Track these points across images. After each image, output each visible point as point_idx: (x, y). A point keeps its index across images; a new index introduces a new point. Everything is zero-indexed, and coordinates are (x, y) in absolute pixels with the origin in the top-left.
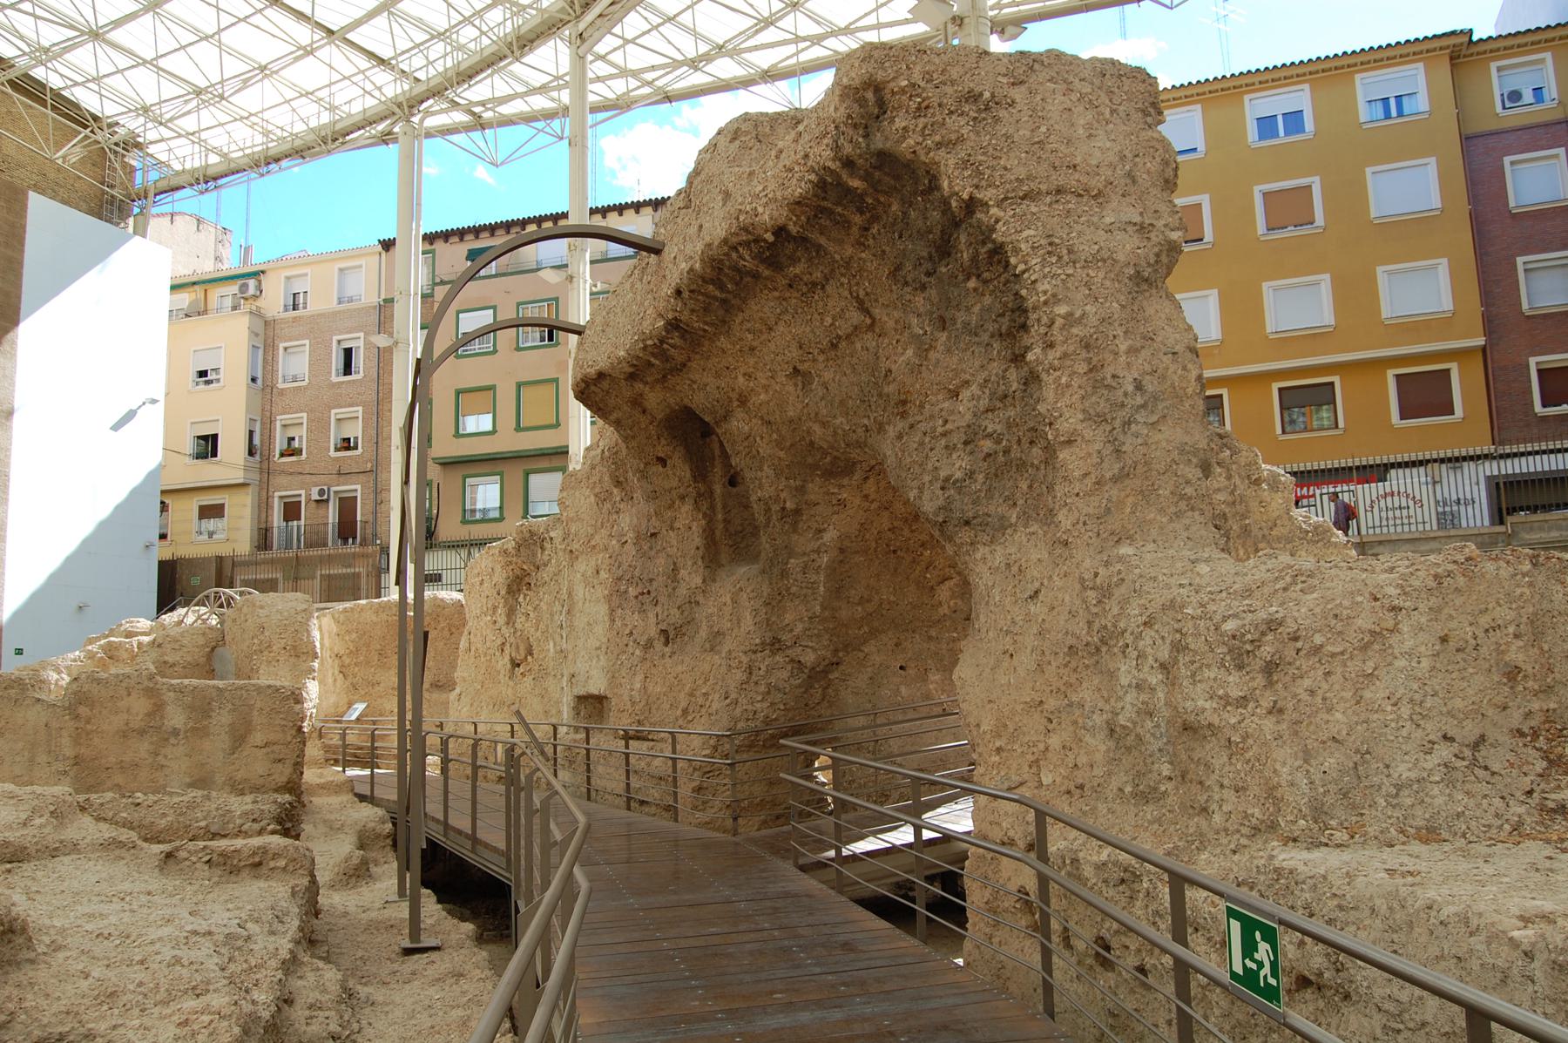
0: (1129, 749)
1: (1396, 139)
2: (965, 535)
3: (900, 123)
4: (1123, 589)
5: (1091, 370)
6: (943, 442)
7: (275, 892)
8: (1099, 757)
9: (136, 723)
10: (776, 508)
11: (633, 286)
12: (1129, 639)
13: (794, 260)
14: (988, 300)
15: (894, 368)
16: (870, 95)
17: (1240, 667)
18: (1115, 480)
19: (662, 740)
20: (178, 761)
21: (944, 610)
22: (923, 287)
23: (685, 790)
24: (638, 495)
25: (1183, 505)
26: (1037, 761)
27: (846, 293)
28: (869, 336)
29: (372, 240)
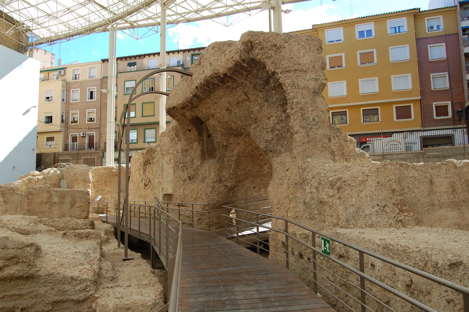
0: (308, 207)
1: (398, 39)
2: (271, 154)
3: (256, 52)
4: (308, 169)
6: (266, 130)
7: (92, 243)
8: (301, 209)
9: (44, 200)
10: (221, 144)
11: (183, 84)
13: (228, 82)
14: (277, 96)
15: (254, 111)
16: (249, 44)
17: (332, 188)
18: (307, 142)
20: (56, 210)
21: (265, 172)
22: (262, 91)
23: (195, 219)
24: (182, 139)
25: (324, 149)
28: (247, 102)
29: (99, 59)
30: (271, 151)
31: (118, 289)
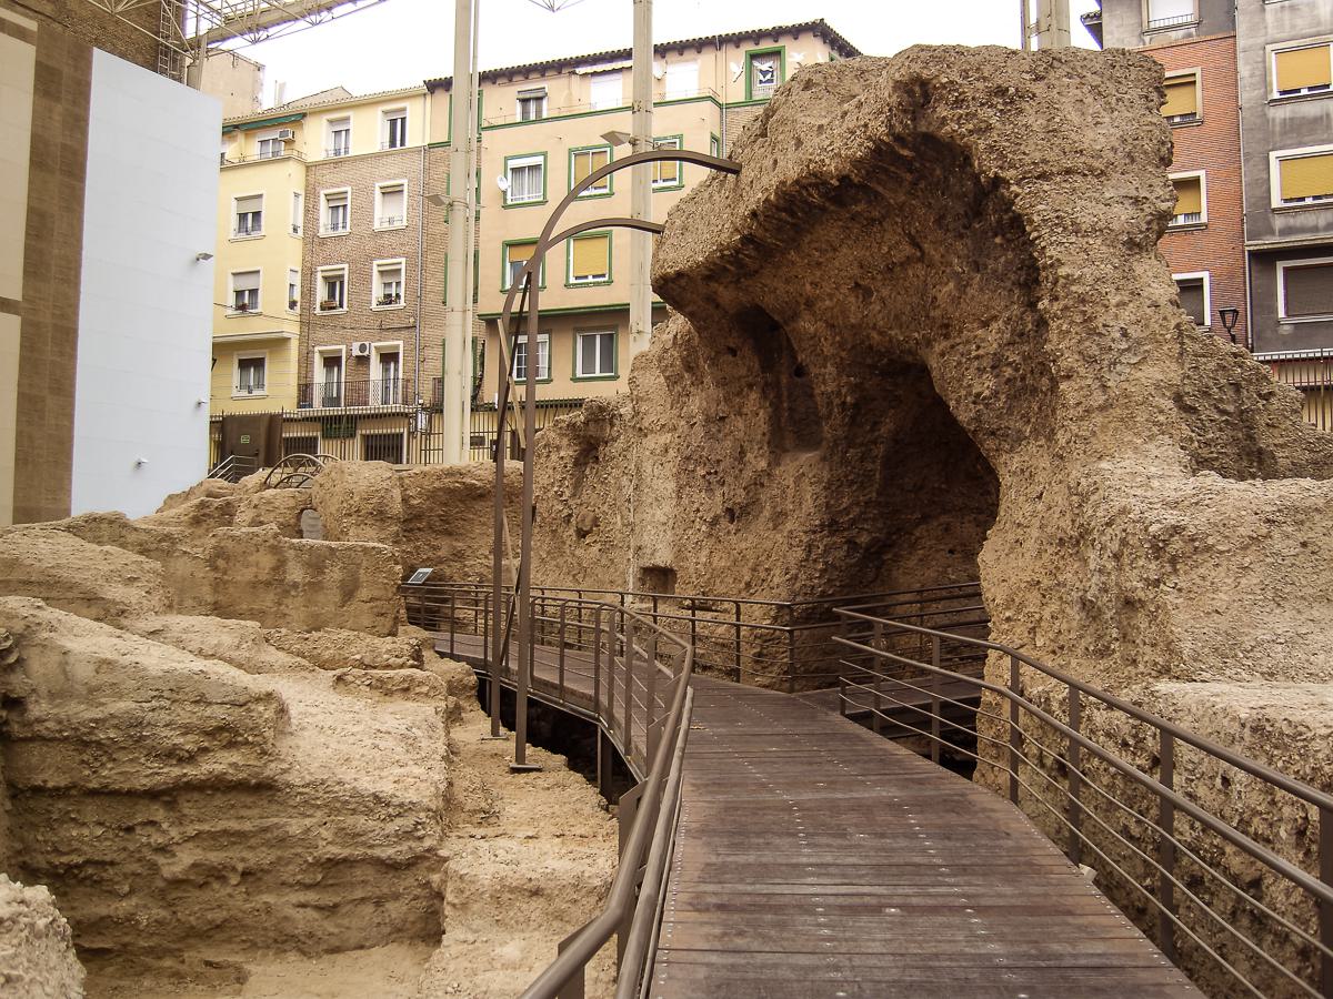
2: (990, 444)
5: (1085, 321)
8: (1075, 624)
9: (263, 577)
10: (837, 401)
12: (1096, 534)
13: (856, 202)
14: (1010, 255)
15: (939, 296)
16: (917, 89)
17: (1157, 558)
18: (1102, 408)
19: (725, 611)
22: (961, 236)
23: (748, 653)
24: (707, 380)
25: (1155, 429)
26: (1034, 628)
27: (900, 230)
28: (919, 266)
30: (993, 433)
31: (501, 842)
